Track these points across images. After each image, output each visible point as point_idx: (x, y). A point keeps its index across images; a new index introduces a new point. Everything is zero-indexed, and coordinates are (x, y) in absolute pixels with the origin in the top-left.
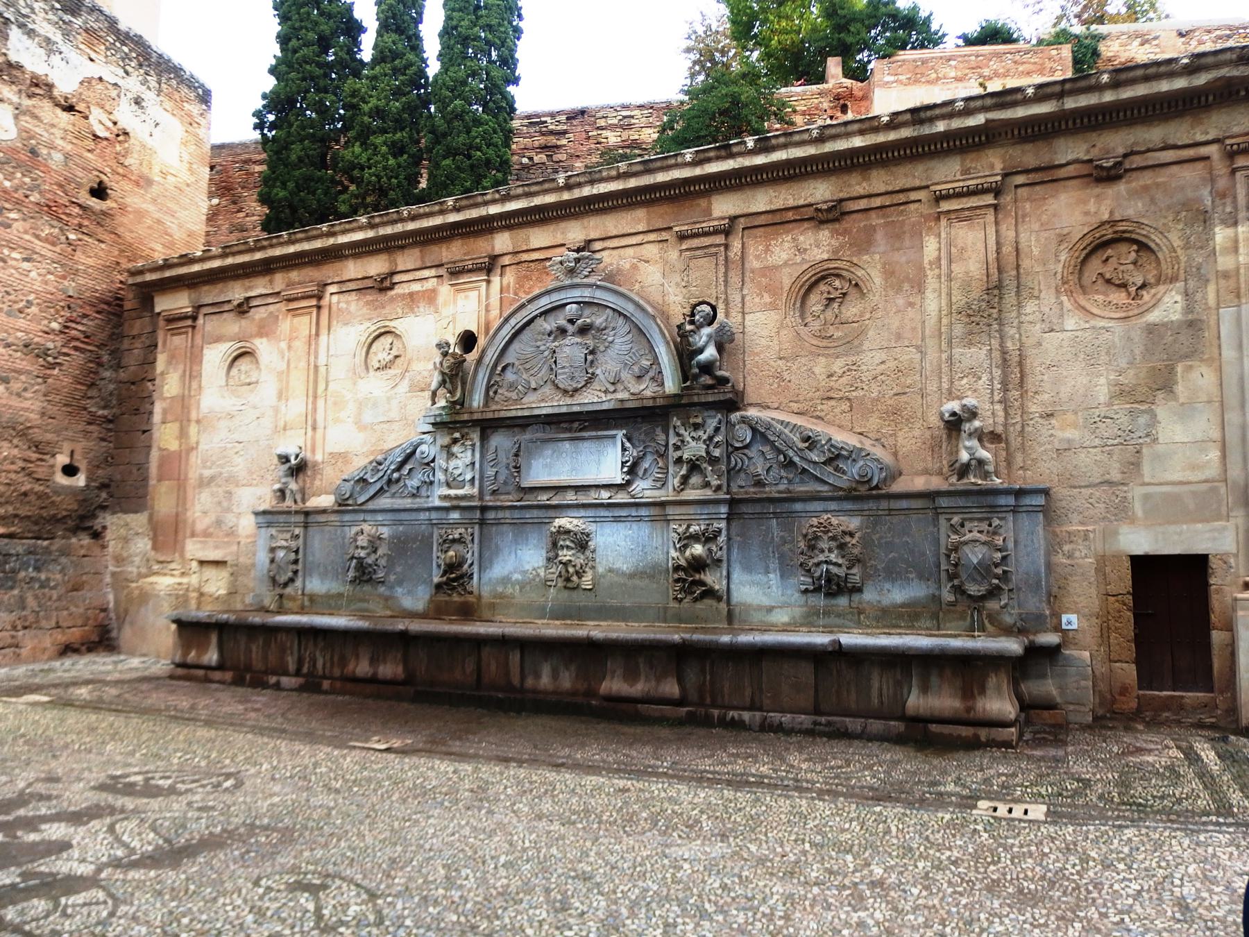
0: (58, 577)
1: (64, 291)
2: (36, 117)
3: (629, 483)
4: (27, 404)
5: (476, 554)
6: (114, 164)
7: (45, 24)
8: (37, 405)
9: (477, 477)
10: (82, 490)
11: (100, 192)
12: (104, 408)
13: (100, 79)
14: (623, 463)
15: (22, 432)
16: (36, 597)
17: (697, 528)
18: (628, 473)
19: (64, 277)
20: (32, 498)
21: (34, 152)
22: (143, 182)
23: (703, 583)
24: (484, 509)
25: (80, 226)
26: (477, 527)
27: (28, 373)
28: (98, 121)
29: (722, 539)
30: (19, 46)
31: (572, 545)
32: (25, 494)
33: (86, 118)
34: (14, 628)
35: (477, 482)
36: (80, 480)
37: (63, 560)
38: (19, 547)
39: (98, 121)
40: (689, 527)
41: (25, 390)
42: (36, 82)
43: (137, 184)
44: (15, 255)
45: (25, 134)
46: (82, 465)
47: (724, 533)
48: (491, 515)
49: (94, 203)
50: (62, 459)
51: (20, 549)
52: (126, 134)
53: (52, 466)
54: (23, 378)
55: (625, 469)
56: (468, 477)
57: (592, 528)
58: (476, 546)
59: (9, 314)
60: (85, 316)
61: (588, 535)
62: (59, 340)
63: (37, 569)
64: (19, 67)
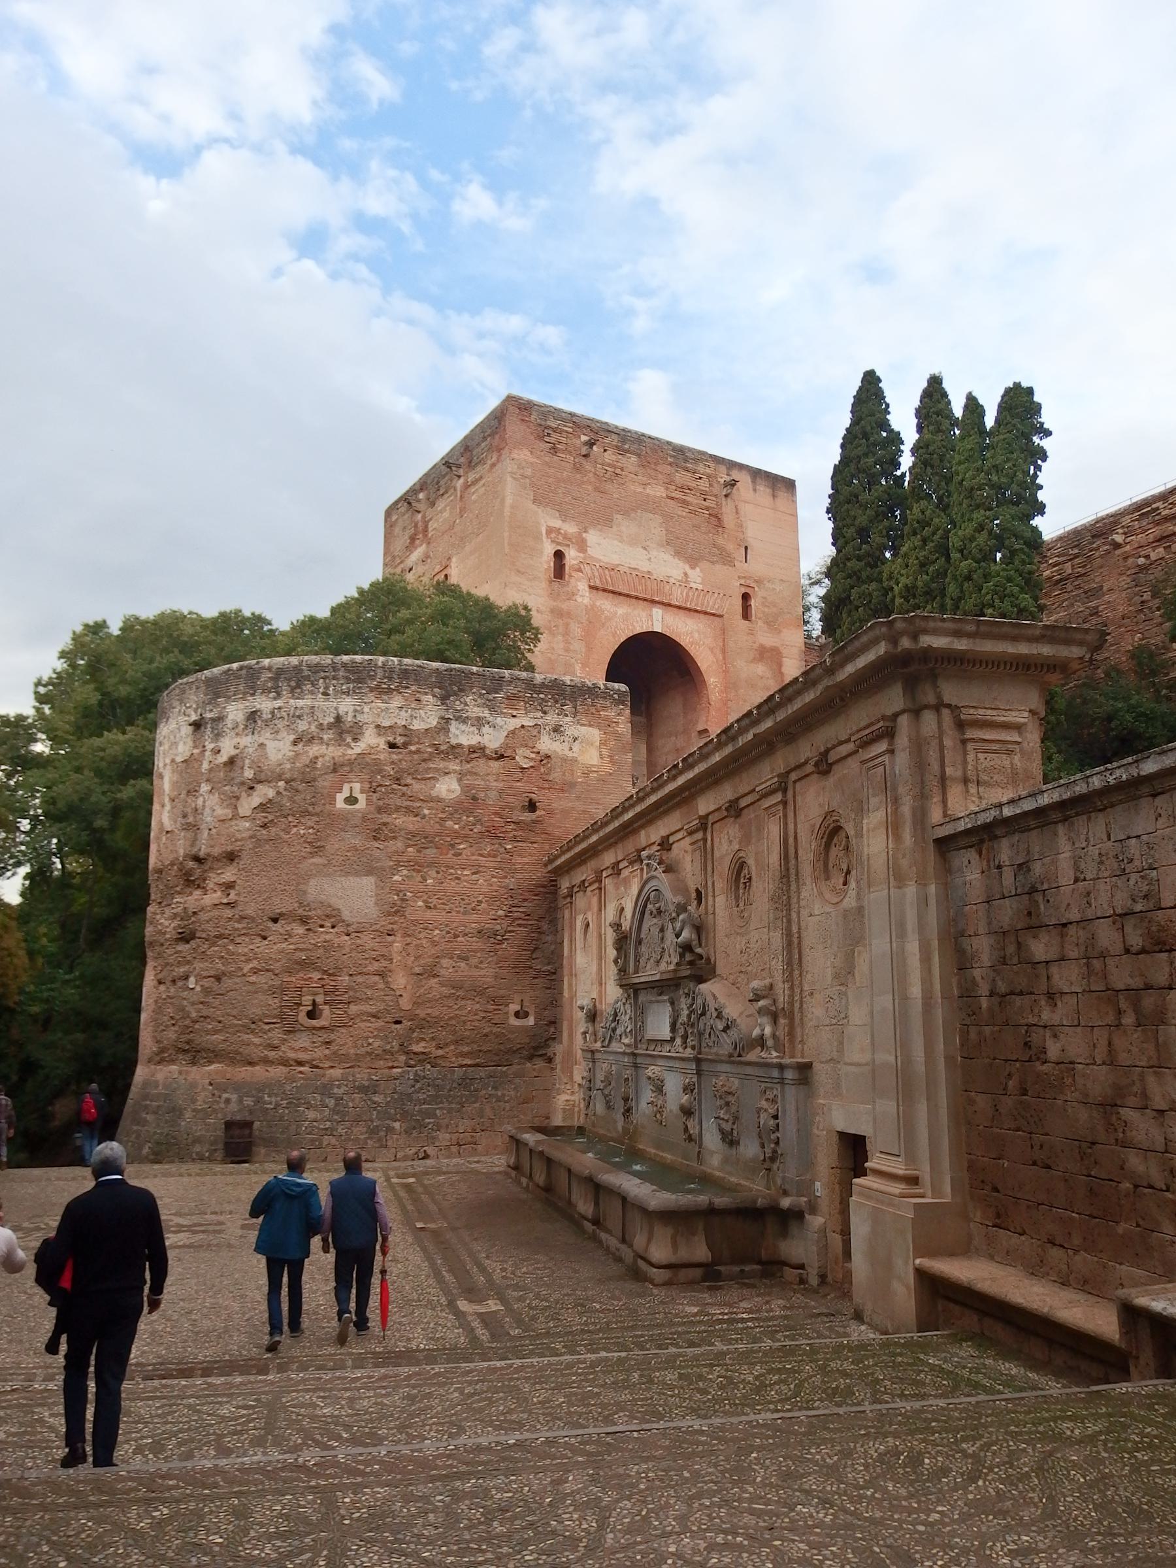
0: (512, 1093)
1: (505, 887)
2: (475, 774)
4: (482, 972)
6: (540, 783)
7: (476, 709)
8: (491, 972)
10: (532, 1027)
11: (532, 806)
12: (548, 964)
13: (523, 726)
15: (479, 992)
16: (493, 1108)
19: (505, 877)
20: (492, 1037)
21: (474, 798)
22: (567, 787)
25: (515, 837)
27: (483, 950)
28: (523, 758)
30: (457, 732)
32: (486, 1035)
33: (514, 758)
34: (474, 1131)
36: (531, 1021)
37: (517, 1080)
38: (482, 1072)
39: (523, 758)
41: (481, 962)
42: (473, 750)
43: (562, 790)
44: (466, 873)
45: (466, 789)
46: (531, 1011)
49: (527, 816)
50: (515, 1007)
51: (483, 1075)
52: (548, 757)
53: (507, 1013)
54: (479, 955)
59: (465, 913)
60: (525, 900)
62: (505, 923)
63: (495, 1088)
64: (459, 746)
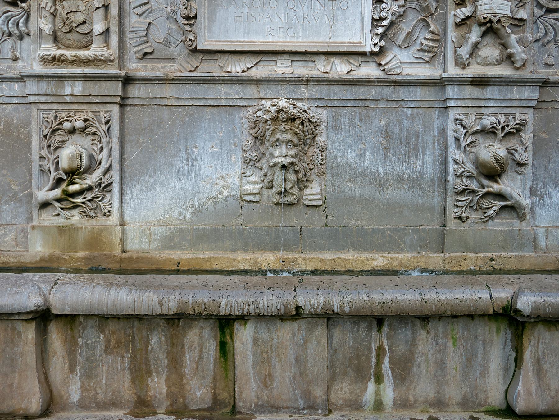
3: (382, 52)
5: (116, 153)
9: (114, 28)
14: (376, 22)
17: (493, 119)
18: (383, 36)
23: (500, 196)
24: (128, 80)
26: (115, 109)
29: (527, 135)
31: (296, 140)
35: (114, 39)
40: (479, 117)
47: (530, 125)
48: (136, 91)
55: (380, 30)
56: (98, 28)
57: (322, 115)
58: (115, 140)
61: (316, 125)
